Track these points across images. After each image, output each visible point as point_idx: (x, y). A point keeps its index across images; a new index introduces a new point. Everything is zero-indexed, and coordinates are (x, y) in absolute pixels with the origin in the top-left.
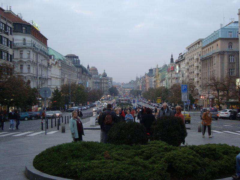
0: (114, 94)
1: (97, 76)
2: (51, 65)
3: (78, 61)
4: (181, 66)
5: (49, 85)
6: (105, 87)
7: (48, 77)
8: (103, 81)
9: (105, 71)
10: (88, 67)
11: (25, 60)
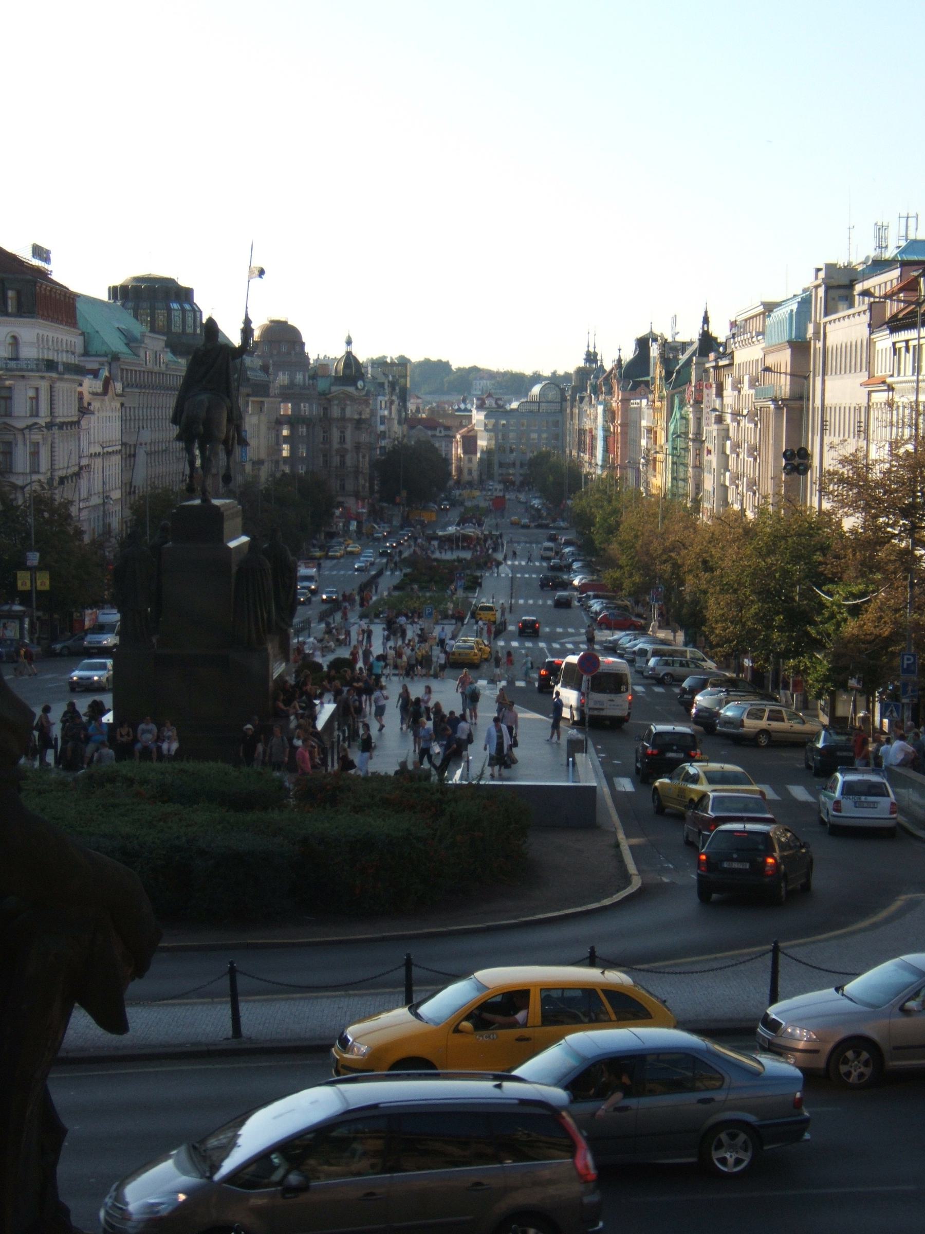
0: (404, 493)
1: (299, 377)
2: (89, 404)
3: (190, 321)
4: (725, 393)
5: (82, 497)
6: (349, 445)
7: (84, 462)
8: (336, 412)
9: (349, 342)
10: (247, 331)
11: (21, 424)
